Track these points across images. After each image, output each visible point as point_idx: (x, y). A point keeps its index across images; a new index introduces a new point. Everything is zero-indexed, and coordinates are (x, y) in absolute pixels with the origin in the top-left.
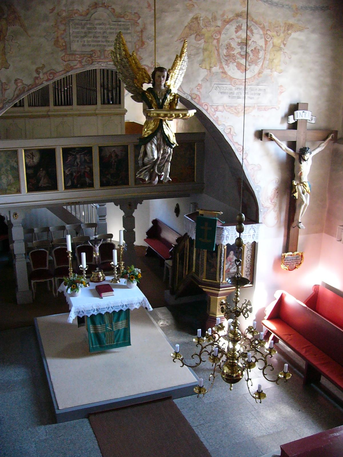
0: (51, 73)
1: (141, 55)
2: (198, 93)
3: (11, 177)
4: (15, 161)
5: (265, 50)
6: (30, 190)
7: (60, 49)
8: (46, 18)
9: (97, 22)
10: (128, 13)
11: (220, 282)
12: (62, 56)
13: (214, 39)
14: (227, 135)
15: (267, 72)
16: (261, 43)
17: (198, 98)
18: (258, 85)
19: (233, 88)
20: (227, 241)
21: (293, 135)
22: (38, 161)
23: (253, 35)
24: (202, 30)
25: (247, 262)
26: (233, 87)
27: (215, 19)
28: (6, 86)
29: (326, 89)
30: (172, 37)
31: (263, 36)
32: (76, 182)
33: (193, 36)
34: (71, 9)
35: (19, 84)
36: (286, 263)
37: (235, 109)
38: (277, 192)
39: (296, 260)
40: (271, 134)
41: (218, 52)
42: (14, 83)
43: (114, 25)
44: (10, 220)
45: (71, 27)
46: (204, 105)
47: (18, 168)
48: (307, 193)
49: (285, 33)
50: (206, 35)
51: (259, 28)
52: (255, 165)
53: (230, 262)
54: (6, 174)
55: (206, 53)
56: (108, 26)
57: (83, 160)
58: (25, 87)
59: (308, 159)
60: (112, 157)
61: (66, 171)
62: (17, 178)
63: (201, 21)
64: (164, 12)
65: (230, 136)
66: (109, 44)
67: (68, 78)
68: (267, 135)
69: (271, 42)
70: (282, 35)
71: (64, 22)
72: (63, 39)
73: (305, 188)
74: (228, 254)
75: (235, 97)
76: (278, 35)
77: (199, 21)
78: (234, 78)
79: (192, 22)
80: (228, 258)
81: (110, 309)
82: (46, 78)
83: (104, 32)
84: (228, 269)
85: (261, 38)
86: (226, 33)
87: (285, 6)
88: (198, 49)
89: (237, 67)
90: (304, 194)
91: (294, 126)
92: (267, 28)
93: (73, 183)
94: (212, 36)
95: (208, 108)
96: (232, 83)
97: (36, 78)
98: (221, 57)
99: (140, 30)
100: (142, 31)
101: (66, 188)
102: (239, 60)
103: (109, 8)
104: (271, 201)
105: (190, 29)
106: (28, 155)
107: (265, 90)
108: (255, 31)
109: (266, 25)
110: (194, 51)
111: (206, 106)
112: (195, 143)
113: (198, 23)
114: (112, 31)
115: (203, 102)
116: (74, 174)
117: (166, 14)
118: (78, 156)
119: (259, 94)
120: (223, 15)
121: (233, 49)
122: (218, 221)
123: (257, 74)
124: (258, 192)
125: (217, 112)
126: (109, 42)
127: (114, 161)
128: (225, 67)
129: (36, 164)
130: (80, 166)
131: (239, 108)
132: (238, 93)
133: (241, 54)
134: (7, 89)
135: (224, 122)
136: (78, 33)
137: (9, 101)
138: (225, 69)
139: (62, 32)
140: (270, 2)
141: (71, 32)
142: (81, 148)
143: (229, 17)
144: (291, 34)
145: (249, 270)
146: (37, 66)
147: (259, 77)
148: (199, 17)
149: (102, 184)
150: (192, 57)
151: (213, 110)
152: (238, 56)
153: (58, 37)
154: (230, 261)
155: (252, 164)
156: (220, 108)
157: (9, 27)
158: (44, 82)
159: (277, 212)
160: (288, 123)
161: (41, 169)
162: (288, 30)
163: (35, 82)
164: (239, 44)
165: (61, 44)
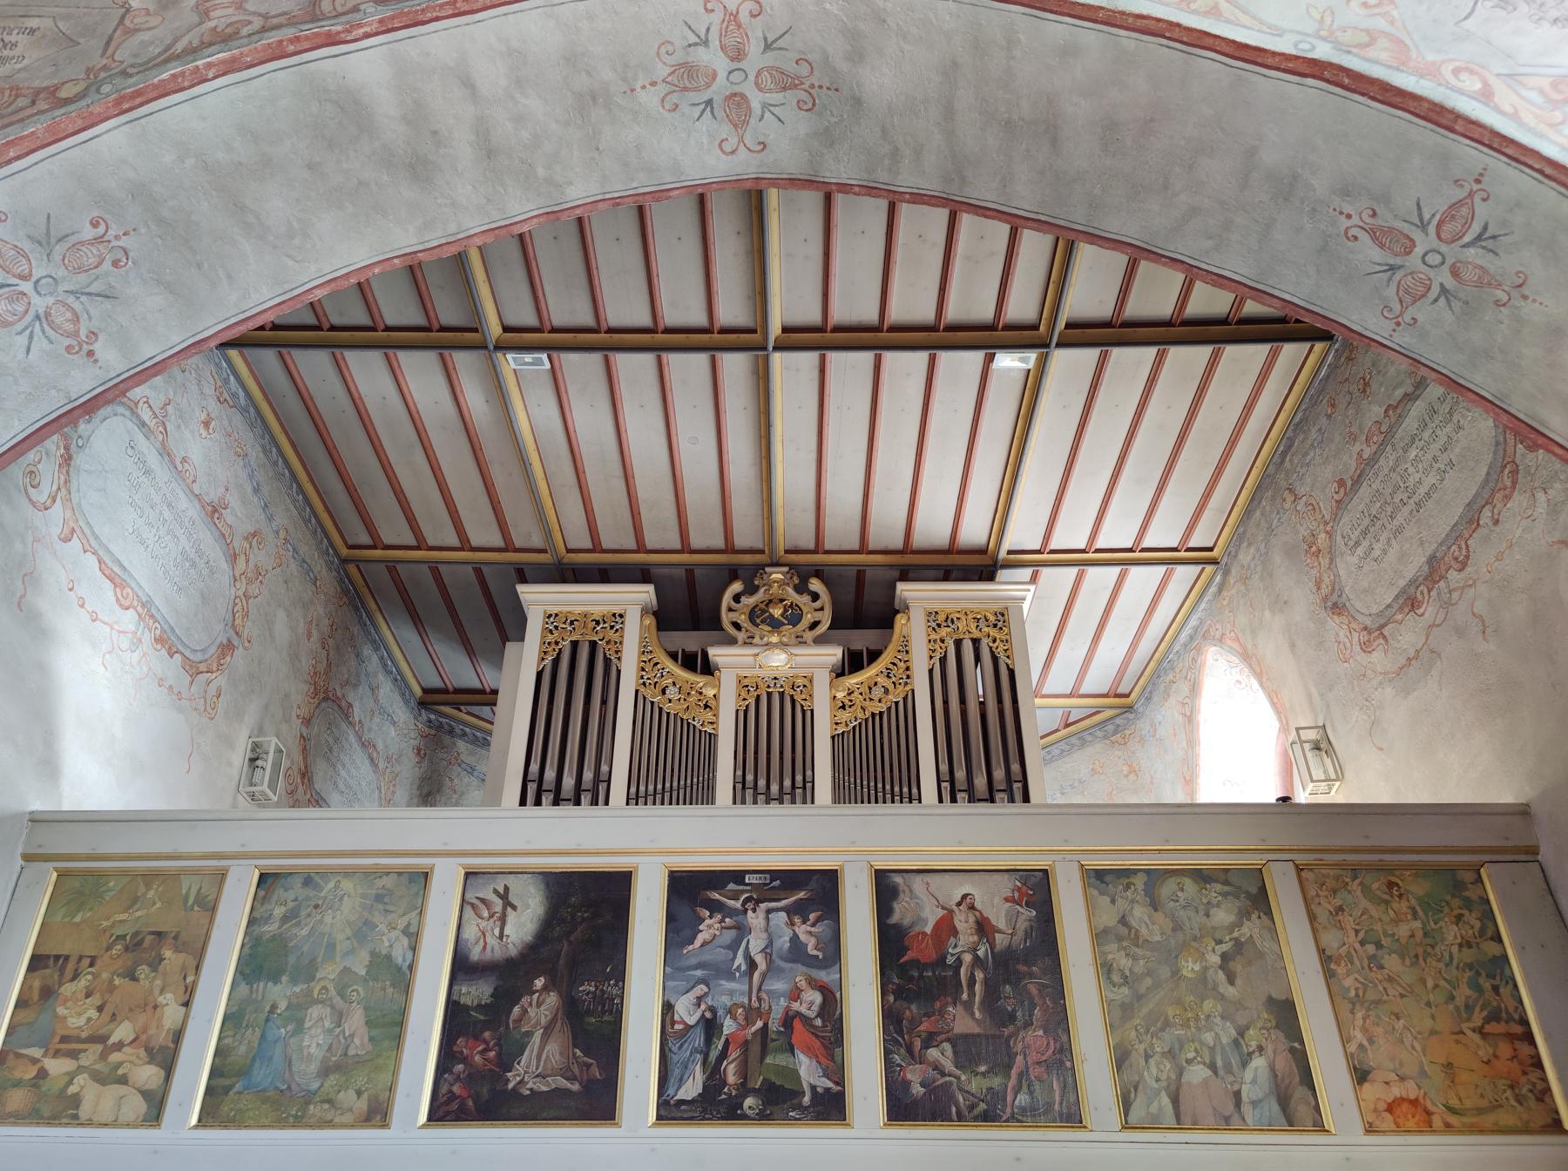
3: (356, 1021)
4: (405, 932)
22: (529, 938)
54: (337, 1000)
57: (784, 942)
60: (955, 932)
101: (670, 1111)
106: (483, 901)
116: (729, 1026)
118: (755, 919)
127: (967, 958)
129: (513, 951)
130: (764, 976)
142: (775, 874)
149: (901, 1108)
161: (539, 983)
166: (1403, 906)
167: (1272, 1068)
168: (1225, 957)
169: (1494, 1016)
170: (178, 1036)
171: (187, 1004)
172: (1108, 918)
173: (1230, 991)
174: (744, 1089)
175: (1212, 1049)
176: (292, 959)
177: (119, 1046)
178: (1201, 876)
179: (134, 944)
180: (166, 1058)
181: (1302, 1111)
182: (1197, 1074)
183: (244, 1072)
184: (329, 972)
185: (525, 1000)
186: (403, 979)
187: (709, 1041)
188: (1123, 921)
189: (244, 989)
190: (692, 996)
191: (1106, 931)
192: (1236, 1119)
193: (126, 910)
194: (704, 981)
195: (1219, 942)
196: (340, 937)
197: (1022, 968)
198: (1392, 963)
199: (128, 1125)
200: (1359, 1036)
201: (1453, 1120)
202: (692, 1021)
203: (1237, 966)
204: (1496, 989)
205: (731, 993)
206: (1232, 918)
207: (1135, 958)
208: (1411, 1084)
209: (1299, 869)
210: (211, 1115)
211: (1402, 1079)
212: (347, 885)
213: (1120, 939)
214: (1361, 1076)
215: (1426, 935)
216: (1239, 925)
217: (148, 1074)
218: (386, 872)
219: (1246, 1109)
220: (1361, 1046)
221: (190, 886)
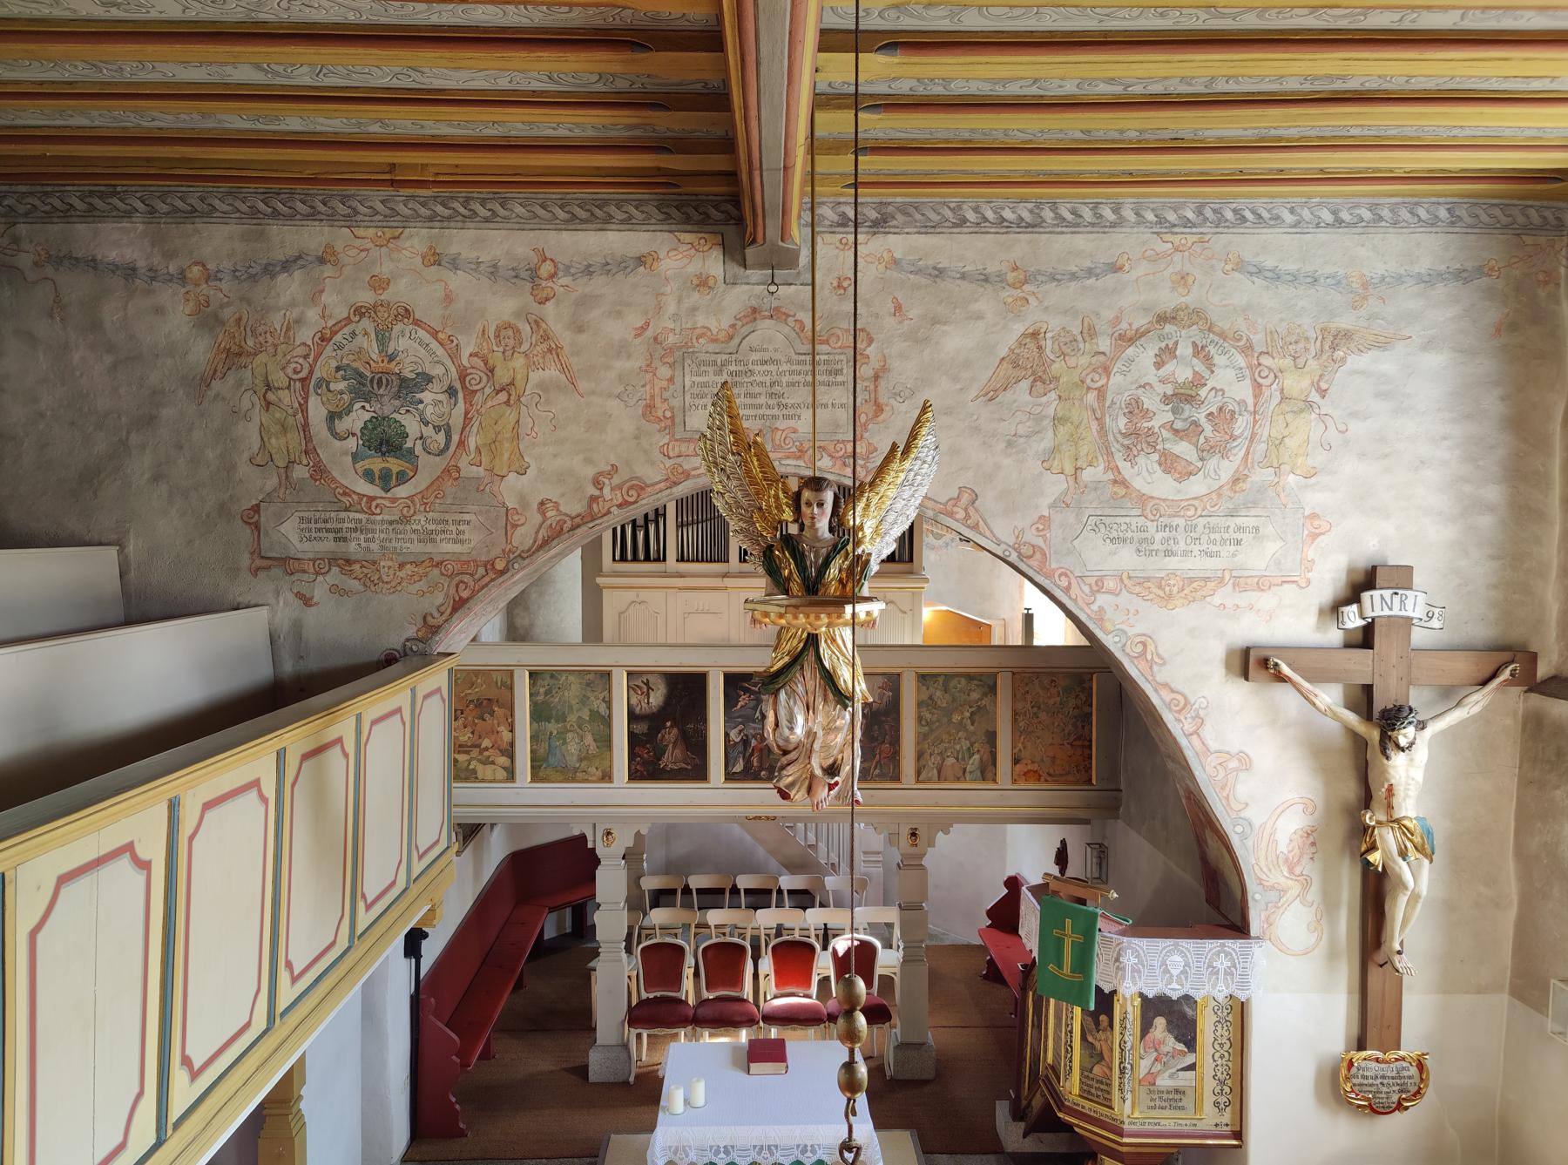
0: (631, 488)
1: (874, 441)
2: (1039, 542)
3: (589, 739)
4: (603, 700)
5: (1255, 412)
6: (634, 776)
7: (658, 427)
8: (622, 350)
9: (755, 356)
10: (839, 332)
11: (1122, 1114)
12: (661, 444)
13: (1089, 388)
14: (1132, 662)
15: (1261, 475)
16: (1244, 391)
17: (1038, 556)
18: (1231, 514)
19: (1152, 527)
20: (1135, 984)
21: (1360, 665)
23: (1213, 372)
24: (1050, 366)
25: (1215, 1061)
26: (1149, 523)
27: (1090, 332)
28: (516, 517)
29: (1486, 521)
30: (962, 389)
31: (1247, 373)
32: (755, 764)
33: (1025, 384)
34: (689, 326)
35: (549, 514)
36: (1361, 1085)
37: (1160, 587)
38: (1313, 844)
39: (1400, 1078)
40: (1276, 660)
41: (1102, 426)
42: (539, 509)
43: (799, 363)
44: (594, 849)
45: (687, 369)
46: (1057, 578)
47: (610, 716)
48: (1419, 856)
49: (1325, 357)
50: (1064, 379)
51: (1233, 350)
52: (1228, 753)
53: (1155, 1054)
54: (578, 730)
55: (1063, 431)
56: (785, 367)
58: (565, 522)
59: (1412, 744)
61: (733, 734)
62: (606, 742)
63: (1049, 342)
64: (939, 322)
65: (1143, 665)
66: (785, 411)
67: (690, 500)
68: (1264, 663)
69: (1274, 386)
70: (1313, 364)
71: (670, 360)
72: (665, 400)
73: (1408, 838)
74: (1146, 1027)
75: (1157, 551)
76: (1301, 365)
77: (1043, 343)
78: (1152, 498)
79: (1020, 344)
80: (1147, 1038)
81: (765, 1153)
82: (620, 500)
83: (772, 384)
84: (1148, 1073)
85: (1241, 378)
86: (1125, 369)
87: (1322, 280)
88: (1039, 418)
89: (1160, 464)
90: (1404, 860)
91: (1365, 638)
92: (1258, 349)
93: (748, 764)
94: (1083, 382)
95: (1070, 583)
96: (1148, 511)
97: (593, 499)
98: (1111, 438)
99: (871, 373)
100: (876, 377)
101: (730, 777)
102: (1168, 446)
103: (790, 319)
104: (1291, 871)
105: (1016, 365)
106: (637, 686)
107: (1257, 529)
108: (1219, 360)
109: (1258, 339)
110: (1028, 424)
111: (1063, 578)
112: (1092, 674)
113: (1039, 348)
114: (797, 378)
115: (1054, 566)
116: (753, 742)
117: (945, 328)
119: (1238, 543)
120: (1117, 320)
121: (1147, 414)
122: (1103, 916)
123: (1228, 483)
124: (1243, 836)
125: (1098, 596)
126: (786, 406)
128: (1124, 466)
129: (655, 710)
131: (1172, 582)
132: (1166, 541)
133: (1174, 426)
134: (517, 526)
135: (1123, 623)
136: (705, 385)
137: (524, 555)
138: (1123, 473)
139: (665, 384)
140: (1269, 274)
141: (688, 383)
143: (1135, 327)
144: (1344, 360)
145: (1227, 1089)
146: (596, 470)
147: (1235, 492)
148: (1043, 330)
150: (1022, 440)
151: (1086, 589)
152: (1166, 434)
153: (653, 397)
154: (1156, 1050)
155: (1216, 752)
156: (1110, 584)
157: (531, 374)
158: (612, 510)
159: (1315, 906)
160: (1341, 626)
161: (668, 724)
162: (1334, 348)
163: (590, 507)
164: (1166, 399)
165: (660, 414)
166: (1053, 691)
167: (981, 759)
168: (972, 714)
169: (1078, 738)
170: (512, 744)
171: (511, 731)
172: (925, 697)
173: (972, 728)
174: (761, 768)
175: (958, 752)
176: (554, 713)
177: (486, 749)
178: (969, 677)
179: (479, 704)
180: (510, 752)
181: (989, 775)
182: (951, 761)
183: (545, 760)
184: (572, 718)
185: (663, 731)
186: (607, 722)
187: (745, 749)
188: (931, 698)
189: (535, 725)
190: (736, 730)
191: (922, 702)
192: (962, 779)
193: (470, 688)
194: (741, 723)
195: (971, 707)
196: (574, 702)
197: (884, 718)
198: (1043, 716)
199: (500, 781)
200: (1020, 746)
201: (1049, 779)
202: (737, 740)
203: (977, 718)
204: (1083, 727)
205: (755, 729)
206: (979, 696)
207: (933, 714)
208: (1036, 765)
209: (1014, 674)
210: (536, 777)
211: (1033, 762)
212: (571, 678)
213: (928, 706)
214: (1016, 761)
215: (1061, 704)
216: (982, 699)
217: (503, 760)
218: (590, 672)
219: (967, 775)
220: (1020, 750)
221: (497, 677)
